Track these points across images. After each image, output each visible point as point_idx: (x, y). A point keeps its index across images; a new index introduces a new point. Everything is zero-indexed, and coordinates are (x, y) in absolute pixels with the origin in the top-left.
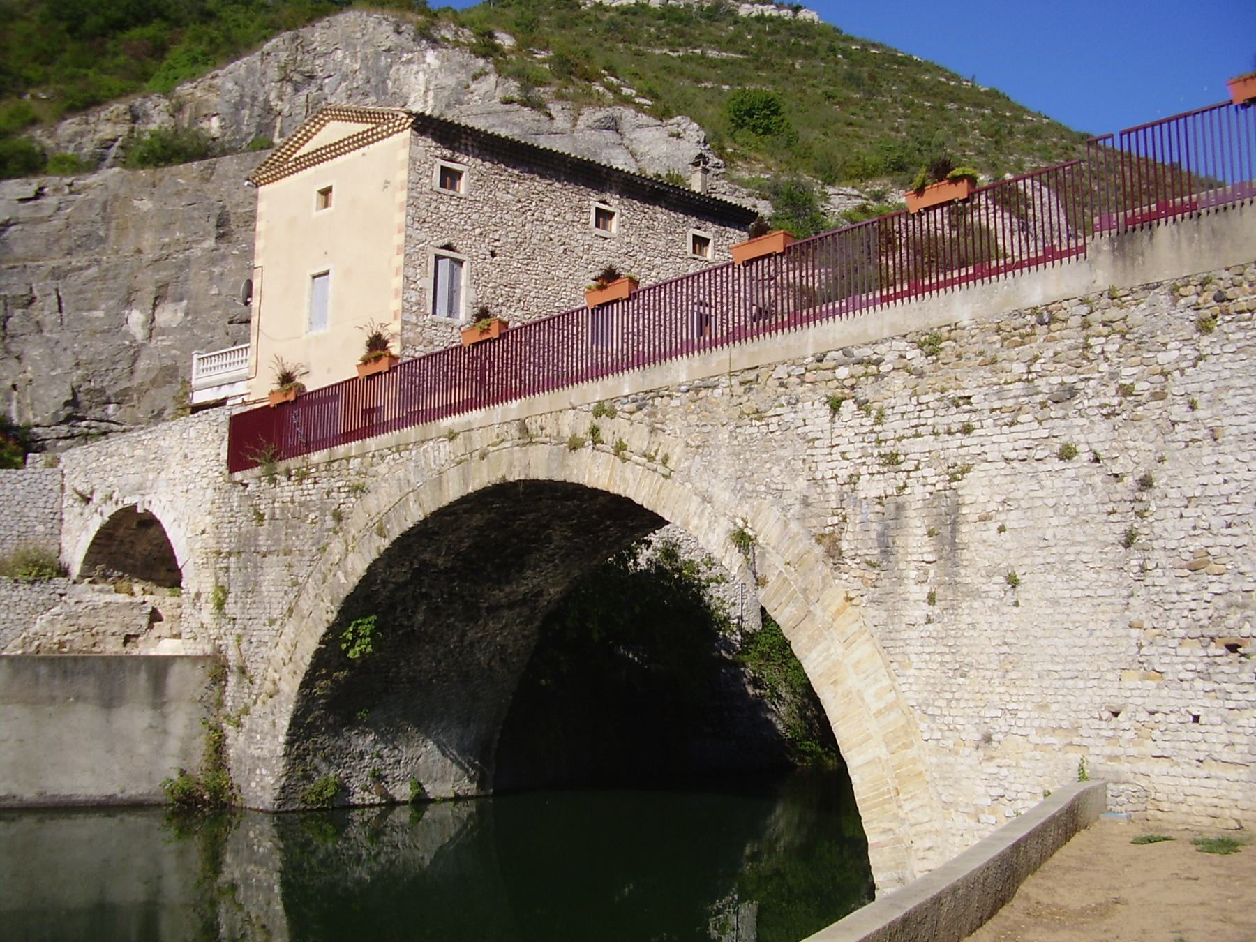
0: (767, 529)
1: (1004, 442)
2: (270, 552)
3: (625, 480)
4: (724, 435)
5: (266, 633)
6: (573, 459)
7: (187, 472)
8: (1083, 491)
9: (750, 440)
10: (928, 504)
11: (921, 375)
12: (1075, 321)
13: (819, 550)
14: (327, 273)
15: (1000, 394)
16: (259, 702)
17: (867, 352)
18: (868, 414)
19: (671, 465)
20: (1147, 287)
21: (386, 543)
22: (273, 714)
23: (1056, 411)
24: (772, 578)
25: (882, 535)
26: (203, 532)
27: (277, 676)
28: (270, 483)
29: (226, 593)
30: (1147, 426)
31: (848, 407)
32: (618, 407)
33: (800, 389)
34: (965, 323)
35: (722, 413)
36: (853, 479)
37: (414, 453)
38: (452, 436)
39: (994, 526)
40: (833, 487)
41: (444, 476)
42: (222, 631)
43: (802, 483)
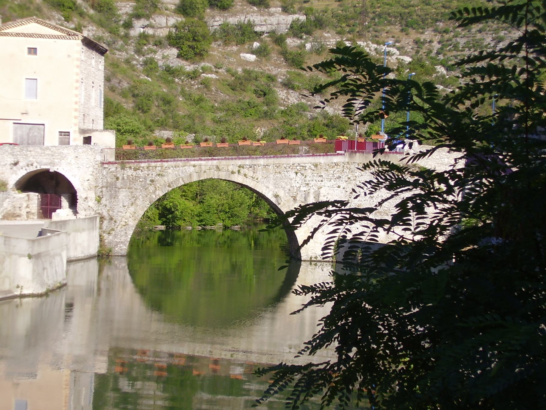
0: (281, 193)
1: (329, 184)
2: (121, 188)
3: (247, 182)
4: (272, 176)
5: (122, 209)
6: (232, 176)
7: (78, 162)
8: (341, 193)
9: (277, 177)
10: (314, 193)
11: (314, 170)
12: (342, 166)
13: (292, 199)
14: (36, 79)
15: (328, 176)
16: (119, 228)
17: (303, 165)
18: (303, 176)
19: (259, 180)
20: (354, 163)
21: (171, 189)
22: (125, 230)
23: (337, 180)
24: (282, 203)
25: (305, 197)
26: (88, 180)
27: (127, 221)
28: (122, 169)
29: (101, 198)
30: (352, 184)
31: (299, 174)
32: (245, 166)
33: (289, 169)
34: (322, 163)
35: (271, 172)
36: (300, 187)
37: (181, 168)
38: (194, 166)
39: (326, 197)
40: (295, 188)
41: (192, 175)
42: (100, 208)
43: (289, 187)
